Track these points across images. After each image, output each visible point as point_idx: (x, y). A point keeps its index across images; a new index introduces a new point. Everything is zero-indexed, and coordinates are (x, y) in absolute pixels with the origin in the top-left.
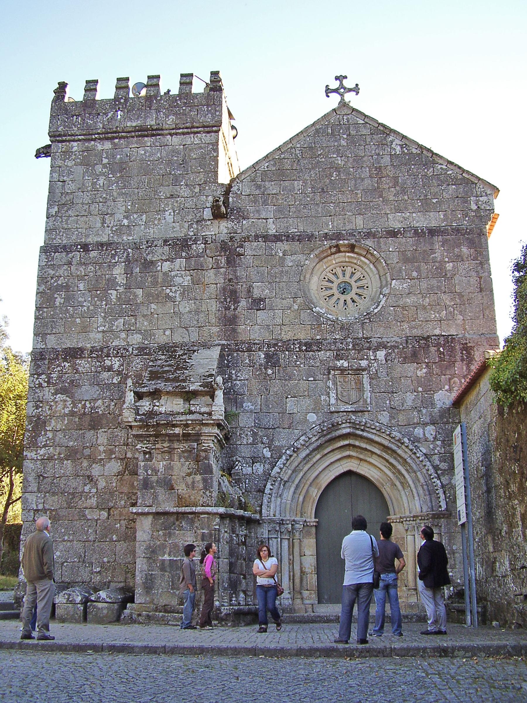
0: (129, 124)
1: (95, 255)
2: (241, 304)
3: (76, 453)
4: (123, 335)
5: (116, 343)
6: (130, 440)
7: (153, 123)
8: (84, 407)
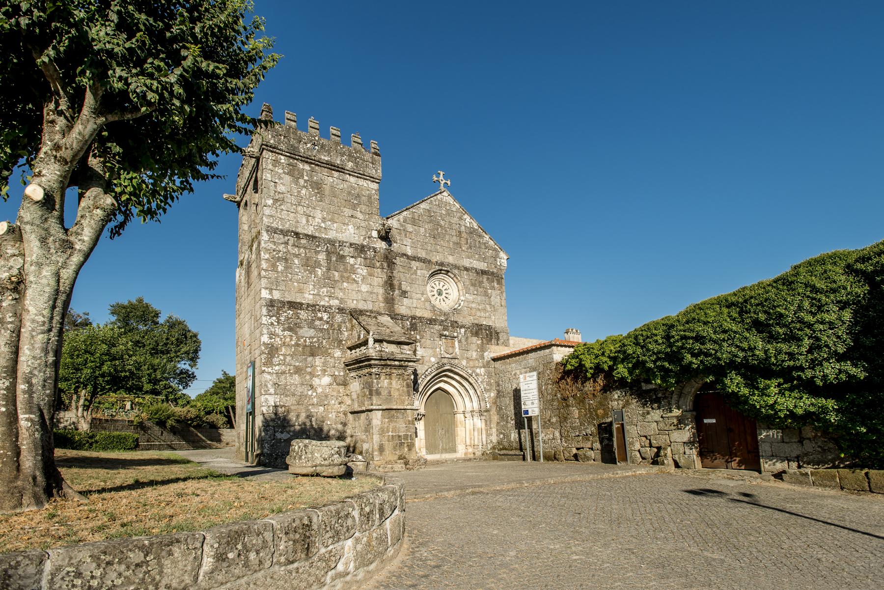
0: (323, 157)
1: (305, 242)
2: (396, 292)
3: (302, 370)
4: (327, 299)
5: (322, 303)
6: (337, 364)
7: (339, 162)
8: (305, 341)
